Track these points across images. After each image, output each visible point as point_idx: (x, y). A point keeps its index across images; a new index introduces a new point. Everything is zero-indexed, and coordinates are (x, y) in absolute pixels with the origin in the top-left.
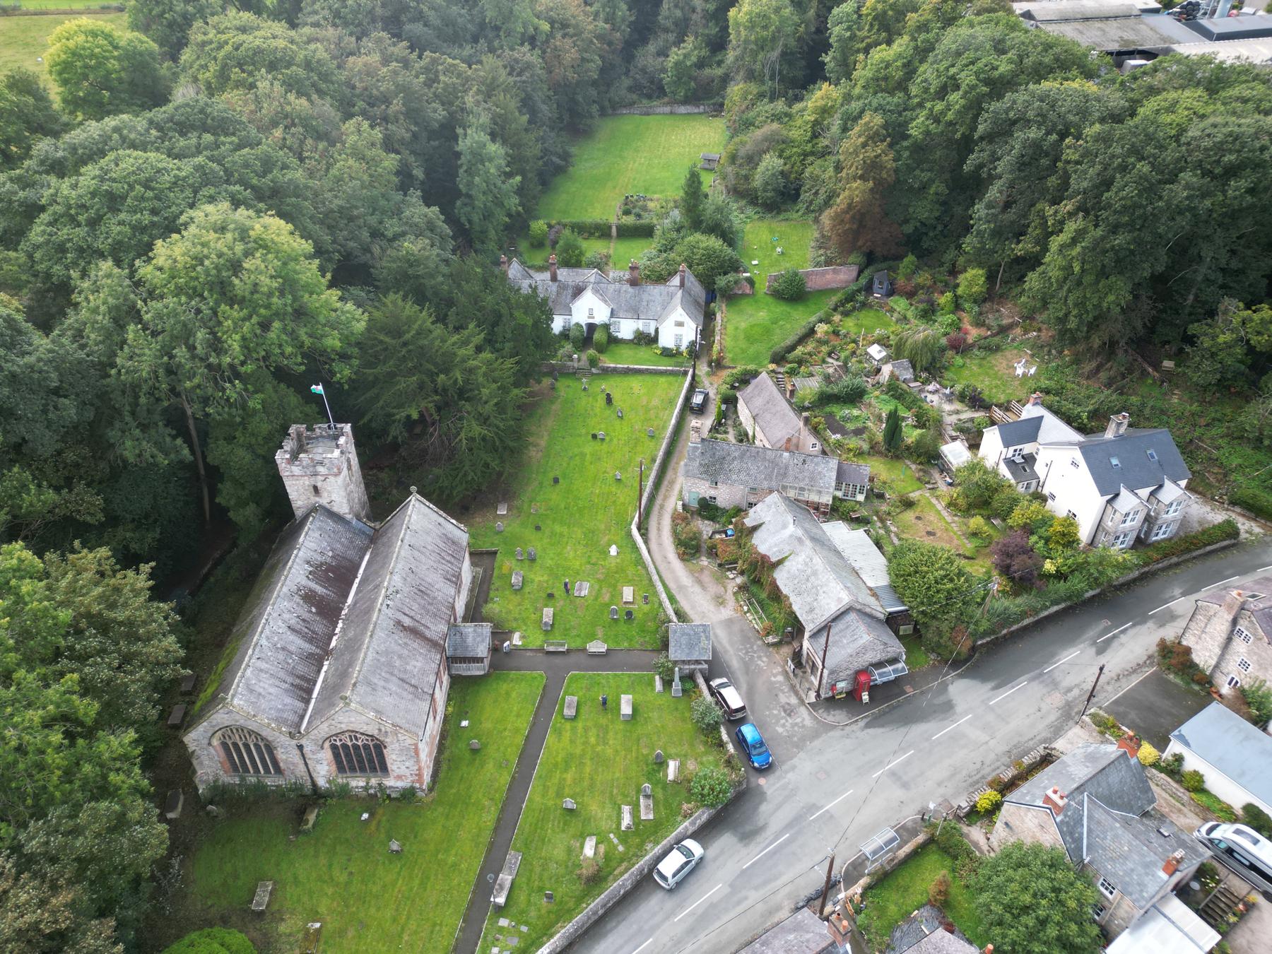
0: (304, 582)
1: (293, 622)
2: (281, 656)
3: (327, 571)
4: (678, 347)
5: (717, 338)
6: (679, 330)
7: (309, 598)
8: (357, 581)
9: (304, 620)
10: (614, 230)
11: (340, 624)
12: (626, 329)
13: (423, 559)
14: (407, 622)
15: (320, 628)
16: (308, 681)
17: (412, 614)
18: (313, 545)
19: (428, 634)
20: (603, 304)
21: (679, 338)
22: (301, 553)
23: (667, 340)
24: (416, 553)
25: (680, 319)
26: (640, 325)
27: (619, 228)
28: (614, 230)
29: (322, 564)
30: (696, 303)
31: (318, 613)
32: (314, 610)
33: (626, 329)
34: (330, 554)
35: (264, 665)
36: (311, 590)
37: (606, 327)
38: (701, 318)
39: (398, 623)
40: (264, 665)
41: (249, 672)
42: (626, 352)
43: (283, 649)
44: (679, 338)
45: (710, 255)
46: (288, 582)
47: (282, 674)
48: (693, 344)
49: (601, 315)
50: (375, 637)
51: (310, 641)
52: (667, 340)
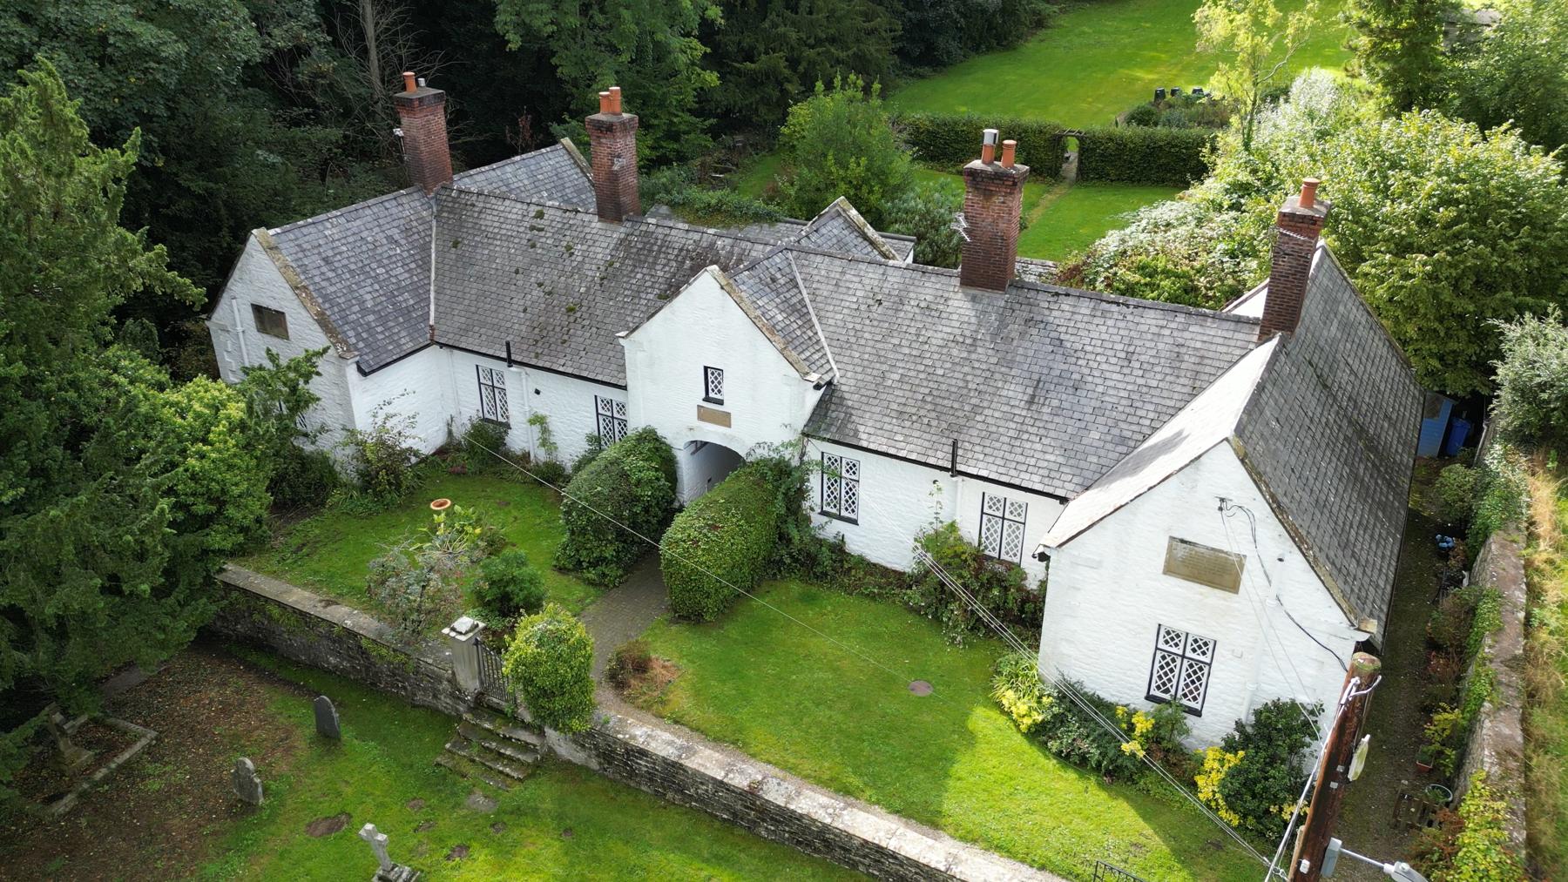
4: (1172, 712)
5: (1496, 731)
6: (1192, 609)
10: (1073, 152)
12: (890, 514)
20: (769, 354)
21: (1183, 662)
23: (1099, 638)
25: (1212, 534)
26: (963, 508)
27: (1089, 146)
28: (1073, 152)
30: (1360, 444)
33: (890, 514)
37: (779, 482)
38: (1380, 557)
42: (830, 643)
44: (1183, 662)
45: (1482, 210)
48: (1276, 729)
49: (767, 412)
52: (1099, 638)
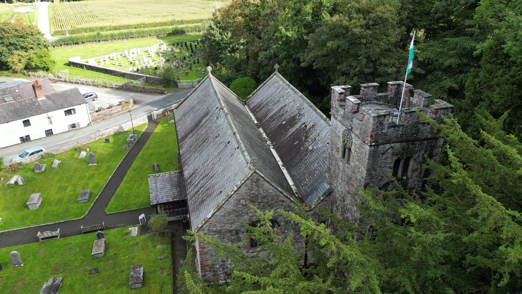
0: (303, 120)
1: (286, 108)
2: (276, 100)
3: (300, 140)
7: (292, 121)
8: (280, 163)
9: (283, 115)
11: (264, 135)
13: (216, 153)
14: (204, 121)
15: (274, 125)
16: (257, 112)
17: (203, 127)
18: (324, 134)
19: (191, 135)
22: (322, 121)
24: (222, 146)
29: (307, 137)
31: (281, 125)
32: (284, 123)
34: (310, 148)
35: (279, 90)
36: (296, 123)
39: (207, 114)
40: (279, 90)
41: (281, 83)
43: (278, 101)
46: (309, 108)
47: (269, 99)
50: (213, 95)
51: (271, 117)
